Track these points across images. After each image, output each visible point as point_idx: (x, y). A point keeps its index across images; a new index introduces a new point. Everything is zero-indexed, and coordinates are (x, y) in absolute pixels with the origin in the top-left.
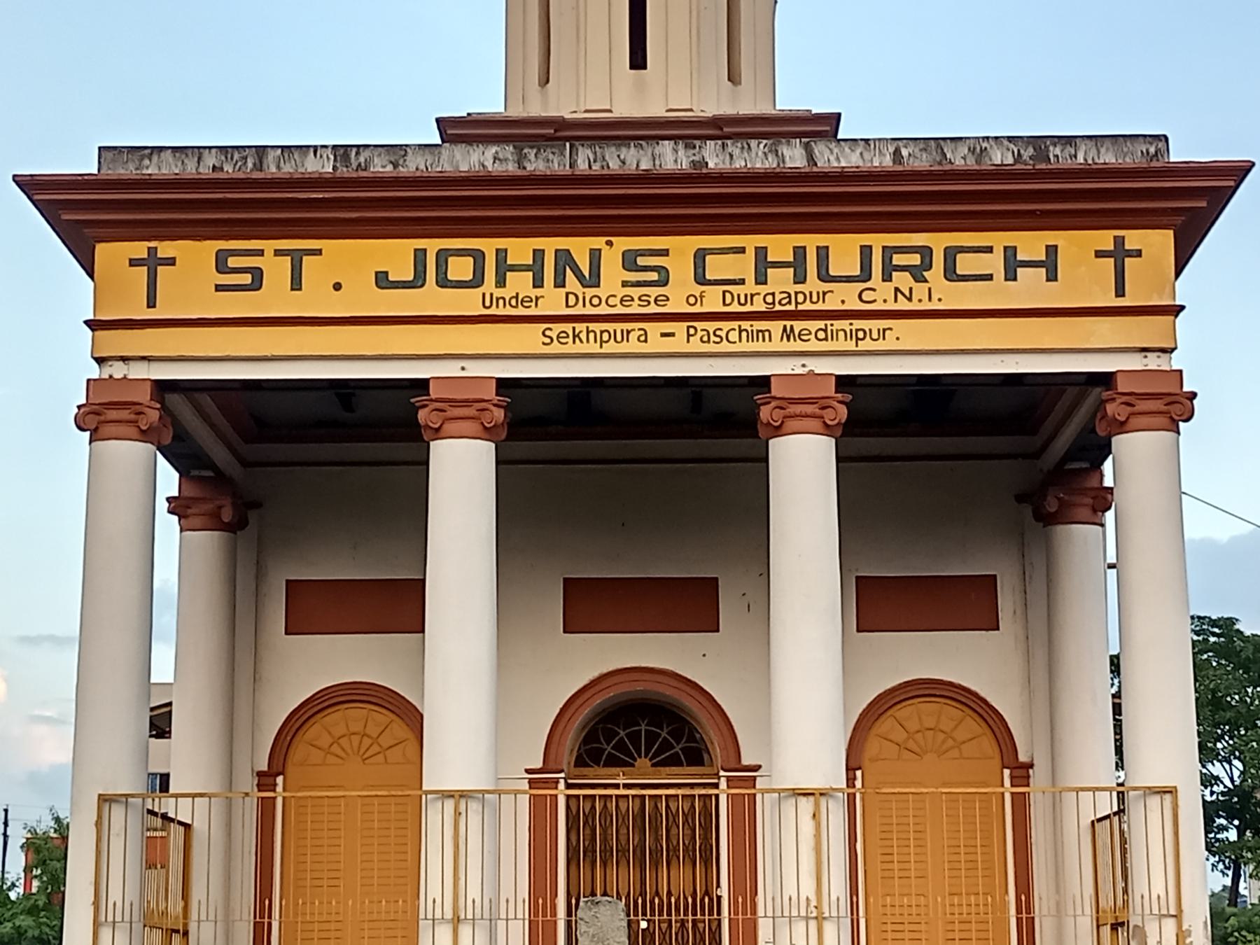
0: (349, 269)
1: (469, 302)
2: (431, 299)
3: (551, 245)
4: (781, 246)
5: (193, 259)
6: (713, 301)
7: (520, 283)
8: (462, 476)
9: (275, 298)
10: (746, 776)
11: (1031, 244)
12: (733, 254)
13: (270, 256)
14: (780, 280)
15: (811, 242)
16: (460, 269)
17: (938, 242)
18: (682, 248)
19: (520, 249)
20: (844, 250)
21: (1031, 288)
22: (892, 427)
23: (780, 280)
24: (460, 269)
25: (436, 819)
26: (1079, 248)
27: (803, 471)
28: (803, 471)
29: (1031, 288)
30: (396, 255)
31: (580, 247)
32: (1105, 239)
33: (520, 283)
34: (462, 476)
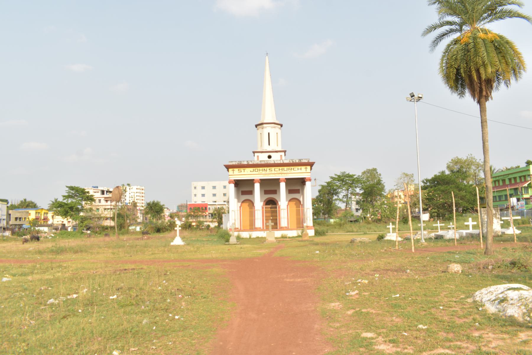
0: (248, 170)
1: (257, 173)
2: (254, 173)
3: (263, 168)
4: (281, 168)
5: (236, 170)
6: (276, 172)
7: (261, 171)
8: (257, 186)
9: (243, 173)
10: (279, 207)
11: (299, 167)
12: (277, 169)
13: (242, 169)
14: (281, 171)
15: (283, 168)
16: (256, 170)
17: (292, 167)
18: (273, 168)
19: (261, 169)
20: (285, 168)
21: (299, 171)
22: (289, 181)
23: (281, 171)
24: (256, 170)
25: (256, 212)
26: (303, 168)
27: (283, 185)
28: (283, 185)
29: (299, 171)
30: (252, 169)
31: (266, 168)
32: (305, 167)
33: (261, 171)
34: (257, 186)
